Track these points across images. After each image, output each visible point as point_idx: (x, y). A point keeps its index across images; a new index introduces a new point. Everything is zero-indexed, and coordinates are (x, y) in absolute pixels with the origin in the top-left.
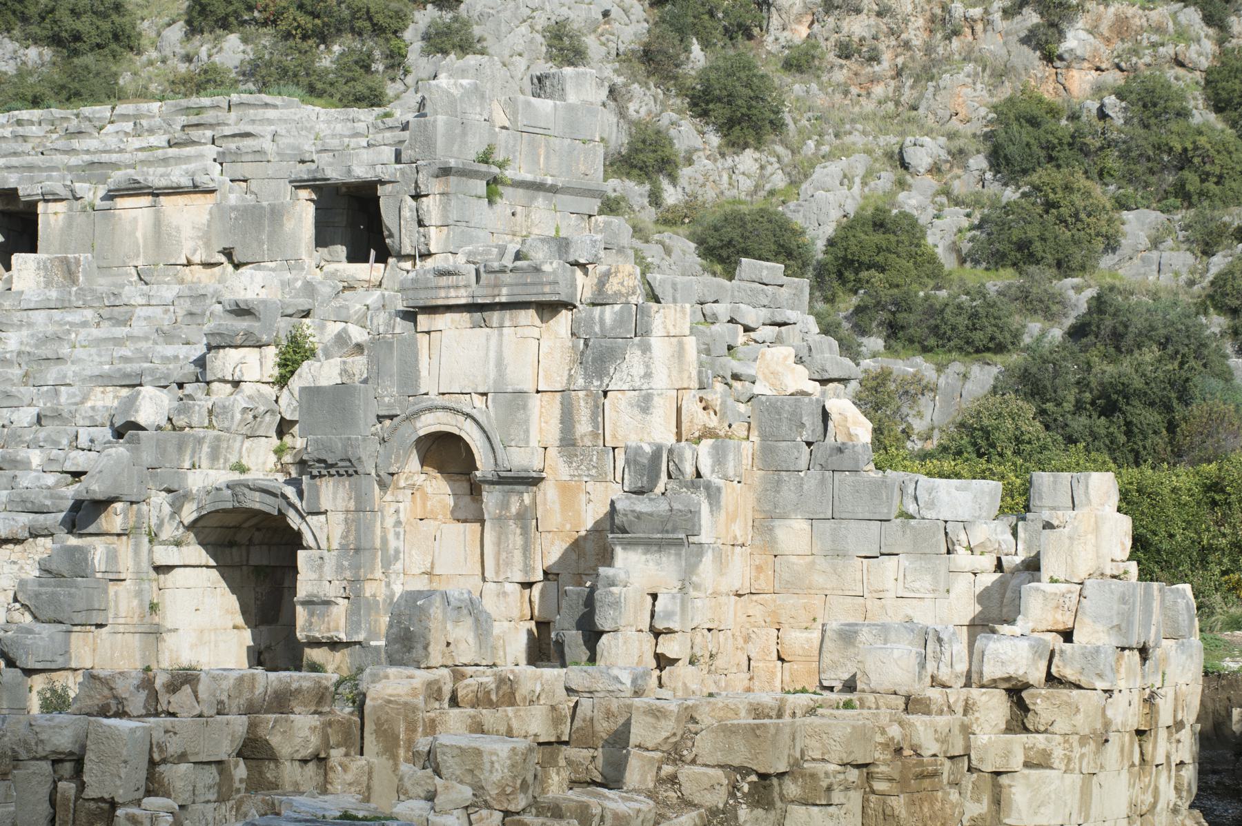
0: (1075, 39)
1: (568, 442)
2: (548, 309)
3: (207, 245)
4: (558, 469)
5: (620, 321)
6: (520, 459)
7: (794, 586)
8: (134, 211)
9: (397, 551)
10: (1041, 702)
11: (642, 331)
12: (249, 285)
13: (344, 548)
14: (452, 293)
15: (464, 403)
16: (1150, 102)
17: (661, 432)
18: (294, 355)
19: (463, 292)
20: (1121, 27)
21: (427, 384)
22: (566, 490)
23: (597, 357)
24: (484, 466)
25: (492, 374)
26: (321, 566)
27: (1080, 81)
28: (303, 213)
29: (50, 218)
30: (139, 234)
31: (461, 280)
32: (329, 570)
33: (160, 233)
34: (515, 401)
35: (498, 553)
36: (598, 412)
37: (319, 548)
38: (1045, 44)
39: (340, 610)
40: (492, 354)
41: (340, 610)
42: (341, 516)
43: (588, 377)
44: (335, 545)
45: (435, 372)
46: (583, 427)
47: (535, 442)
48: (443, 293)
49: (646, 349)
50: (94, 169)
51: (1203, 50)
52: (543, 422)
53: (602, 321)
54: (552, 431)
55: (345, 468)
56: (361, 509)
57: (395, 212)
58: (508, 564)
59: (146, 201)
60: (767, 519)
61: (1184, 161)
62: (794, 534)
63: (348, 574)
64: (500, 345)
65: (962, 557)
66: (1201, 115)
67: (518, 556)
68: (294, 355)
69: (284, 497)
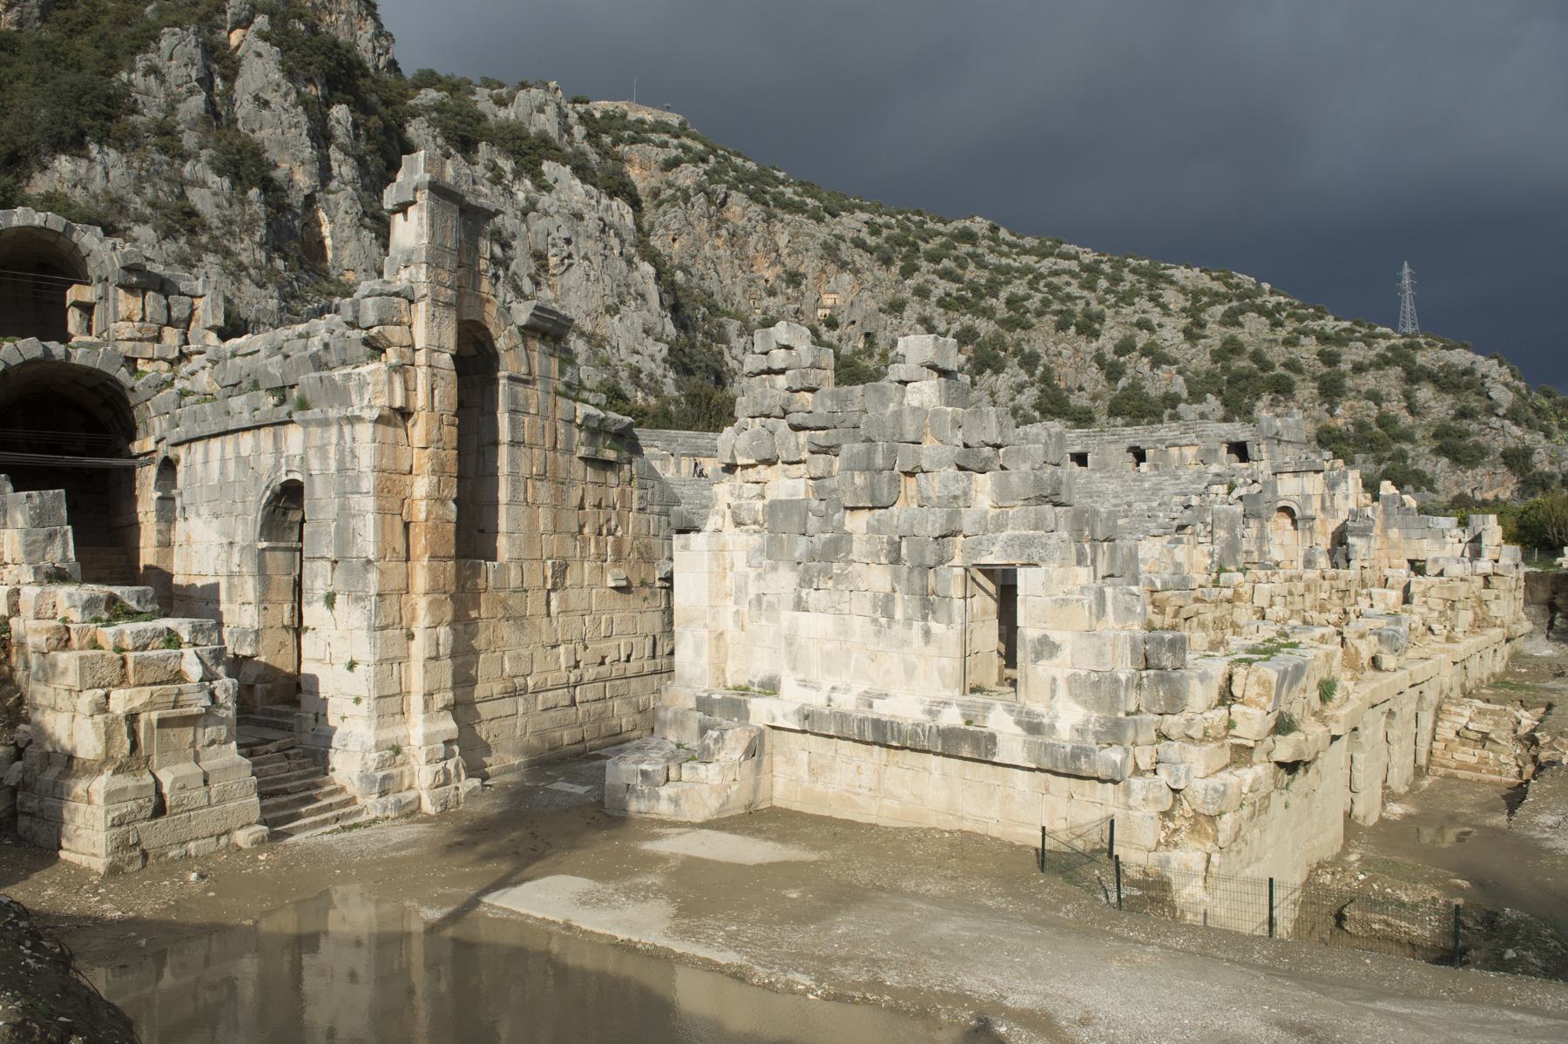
0: (1338, 411)
1: (1323, 508)
2: (1317, 472)
4: (1320, 516)
6: (1309, 512)
7: (1394, 547)
8: (1174, 451)
10: (1494, 580)
11: (1346, 477)
12: (1215, 468)
16: (1361, 426)
17: (1352, 505)
18: (1231, 488)
20: (1352, 407)
21: (1281, 492)
22: (1323, 522)
23: (1332, 485)
27: (1340, 422)
28: (1224, 449)
29: (1150, 453)
33: (1181, 456)
34: (1308, 497)
36: (1332, 500)
38: (1331, 412)
39: (1256, 554)
46: (1328, 504)
47: (1314, 508)
50: (1161, 441)
51: (1375, 412)
52: (1316, 503)
55: (1257, 516)
56: (1262, 528)
57: (1252, 451)
60: (1385, 529)
61: (1372, 441)
62: (1394, 533)
65: (1448, 539)
66: (1376, 429)
68: (1231, 488)
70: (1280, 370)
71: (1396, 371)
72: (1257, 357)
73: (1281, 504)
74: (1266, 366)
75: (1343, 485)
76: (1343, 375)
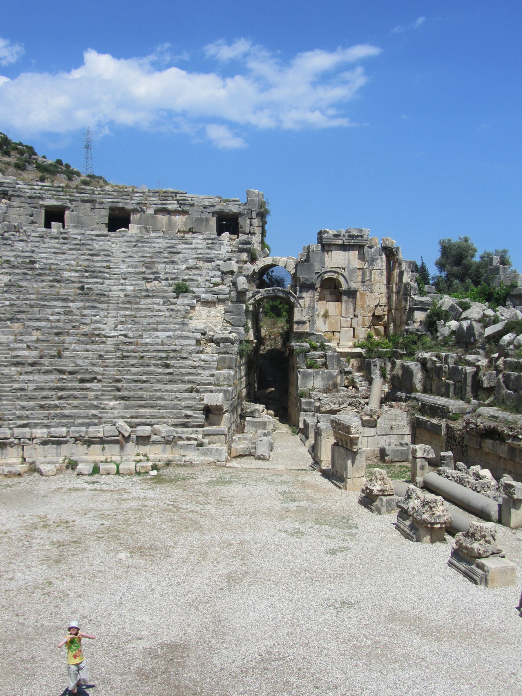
1: (363, 282)
3: (186, 226)
5: (375, 252)
6: (354, 285)
9: (317, 309)
13: (309, 307)
14: (338, 241)
15: (339, 271)
19: (341, 241)
22: (361, 294)
24: (344, 286)
25: (347, 263)
26: (302, 312)
29: (134, 217)
30: (164, 222)
31: (340, 238)
32: (305, 313)
35: (346, 310)
37: (301, 307)
40: (347, 258)
41: (308, 324)
42: (309, 299)
43: (369, 265)
44: (307, 306)
45: (330, 261)
46: (367, 278)
48: (335, 241)
49: (382, 259)
53: (371, 251)
54: (360, 278)
58: (349, 313)
63: (310, 315)
64: (349, 257)
67: (351, 311)
69: (290, 293)
73: (327, 276)
75: (379, 261)
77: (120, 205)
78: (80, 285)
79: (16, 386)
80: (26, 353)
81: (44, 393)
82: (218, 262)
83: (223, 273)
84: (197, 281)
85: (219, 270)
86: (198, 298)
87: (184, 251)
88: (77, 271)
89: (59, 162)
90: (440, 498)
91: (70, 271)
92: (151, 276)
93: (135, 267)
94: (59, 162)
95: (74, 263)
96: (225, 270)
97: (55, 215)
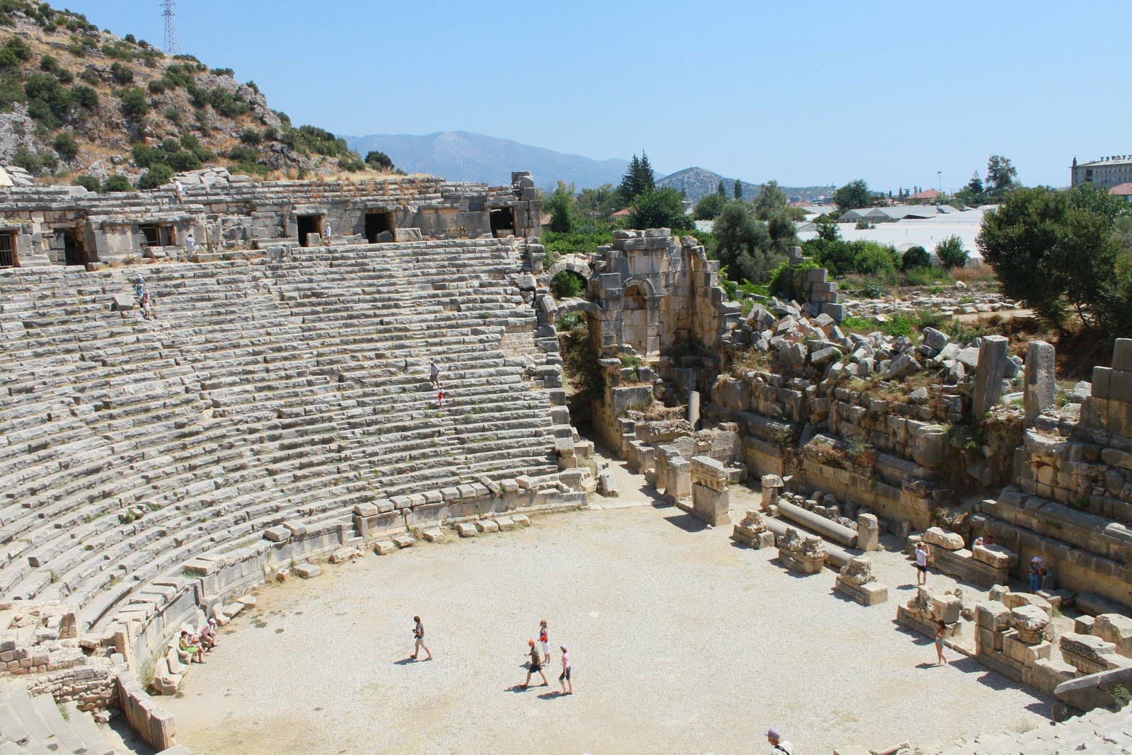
21: (631, 272)
59: (432, 211)
70: (78, 82)
71: (182, 93)
72: (47, 64)
74: (66, 78)
76: (142, 92)
77: (381, 204)
78: (378, 320)
79: (369, 450)
80: (359, 411)
81: (399, 455)
82: (513, 275)
83: (522, 289)
84: (497, 301)
85: (517, 286)
86: (506, 323)
87: (472, 262)
88: (365, 301)
89: (130, 38)
90: (819, 538)
91: (359, 301)
92: (447, 300)
93: (423, 288)
94: (130, 38)
95: (359, 290)
96: (525, 286)
97: (308, 225)
